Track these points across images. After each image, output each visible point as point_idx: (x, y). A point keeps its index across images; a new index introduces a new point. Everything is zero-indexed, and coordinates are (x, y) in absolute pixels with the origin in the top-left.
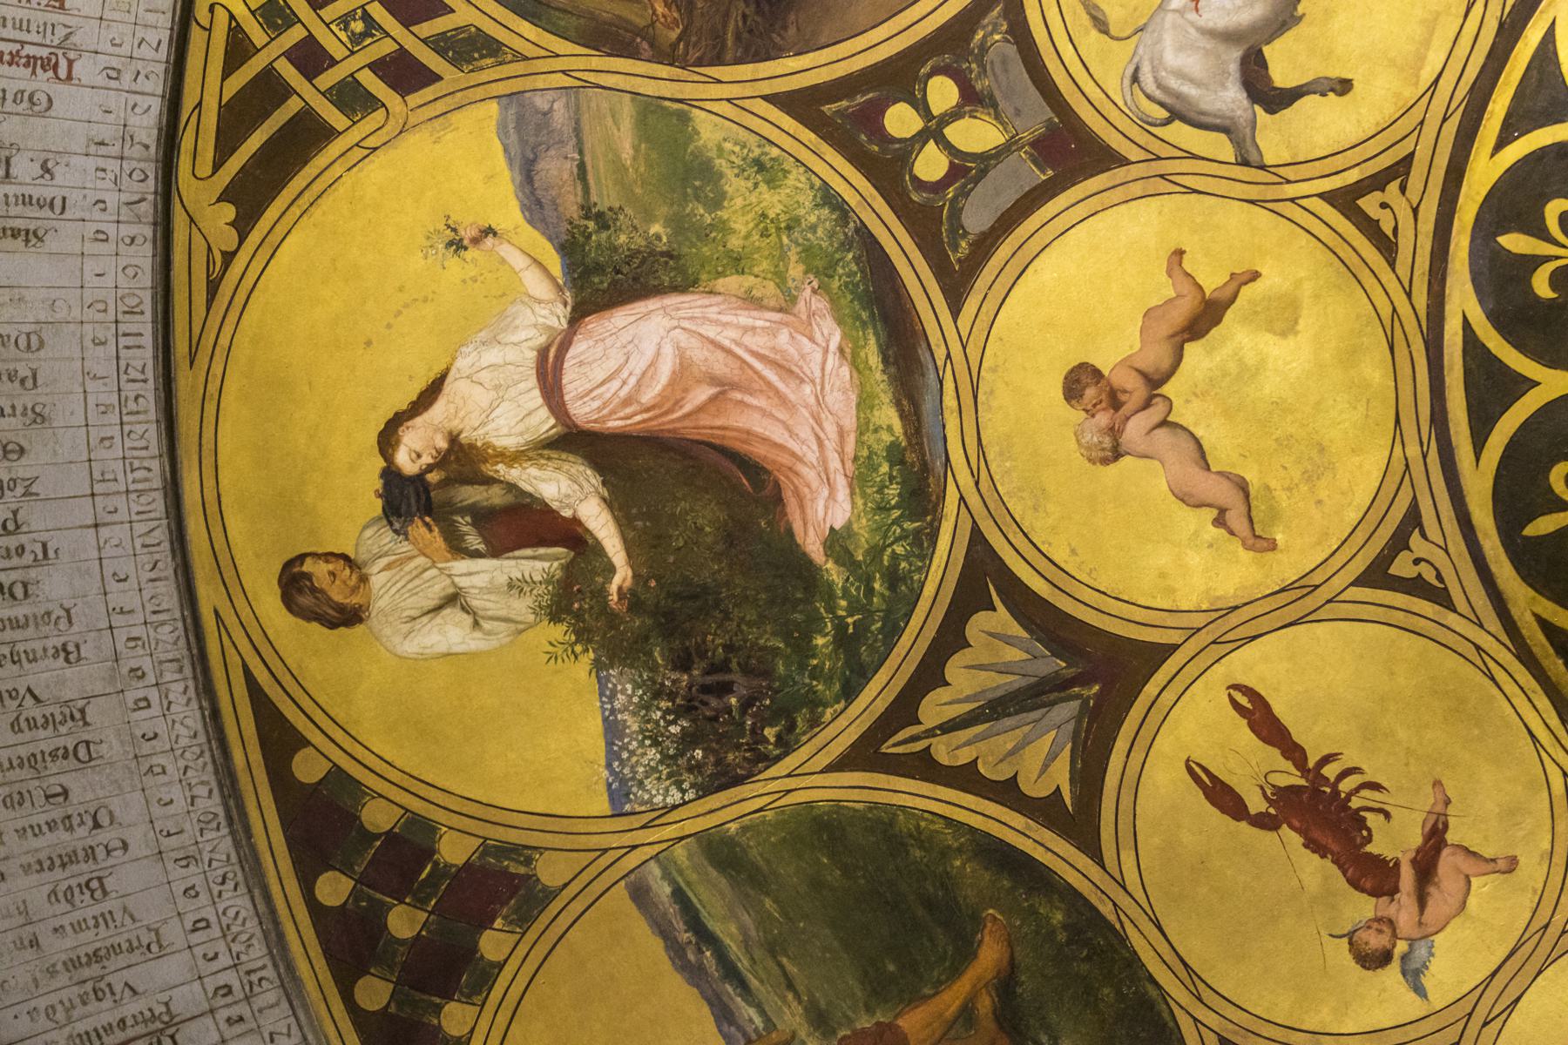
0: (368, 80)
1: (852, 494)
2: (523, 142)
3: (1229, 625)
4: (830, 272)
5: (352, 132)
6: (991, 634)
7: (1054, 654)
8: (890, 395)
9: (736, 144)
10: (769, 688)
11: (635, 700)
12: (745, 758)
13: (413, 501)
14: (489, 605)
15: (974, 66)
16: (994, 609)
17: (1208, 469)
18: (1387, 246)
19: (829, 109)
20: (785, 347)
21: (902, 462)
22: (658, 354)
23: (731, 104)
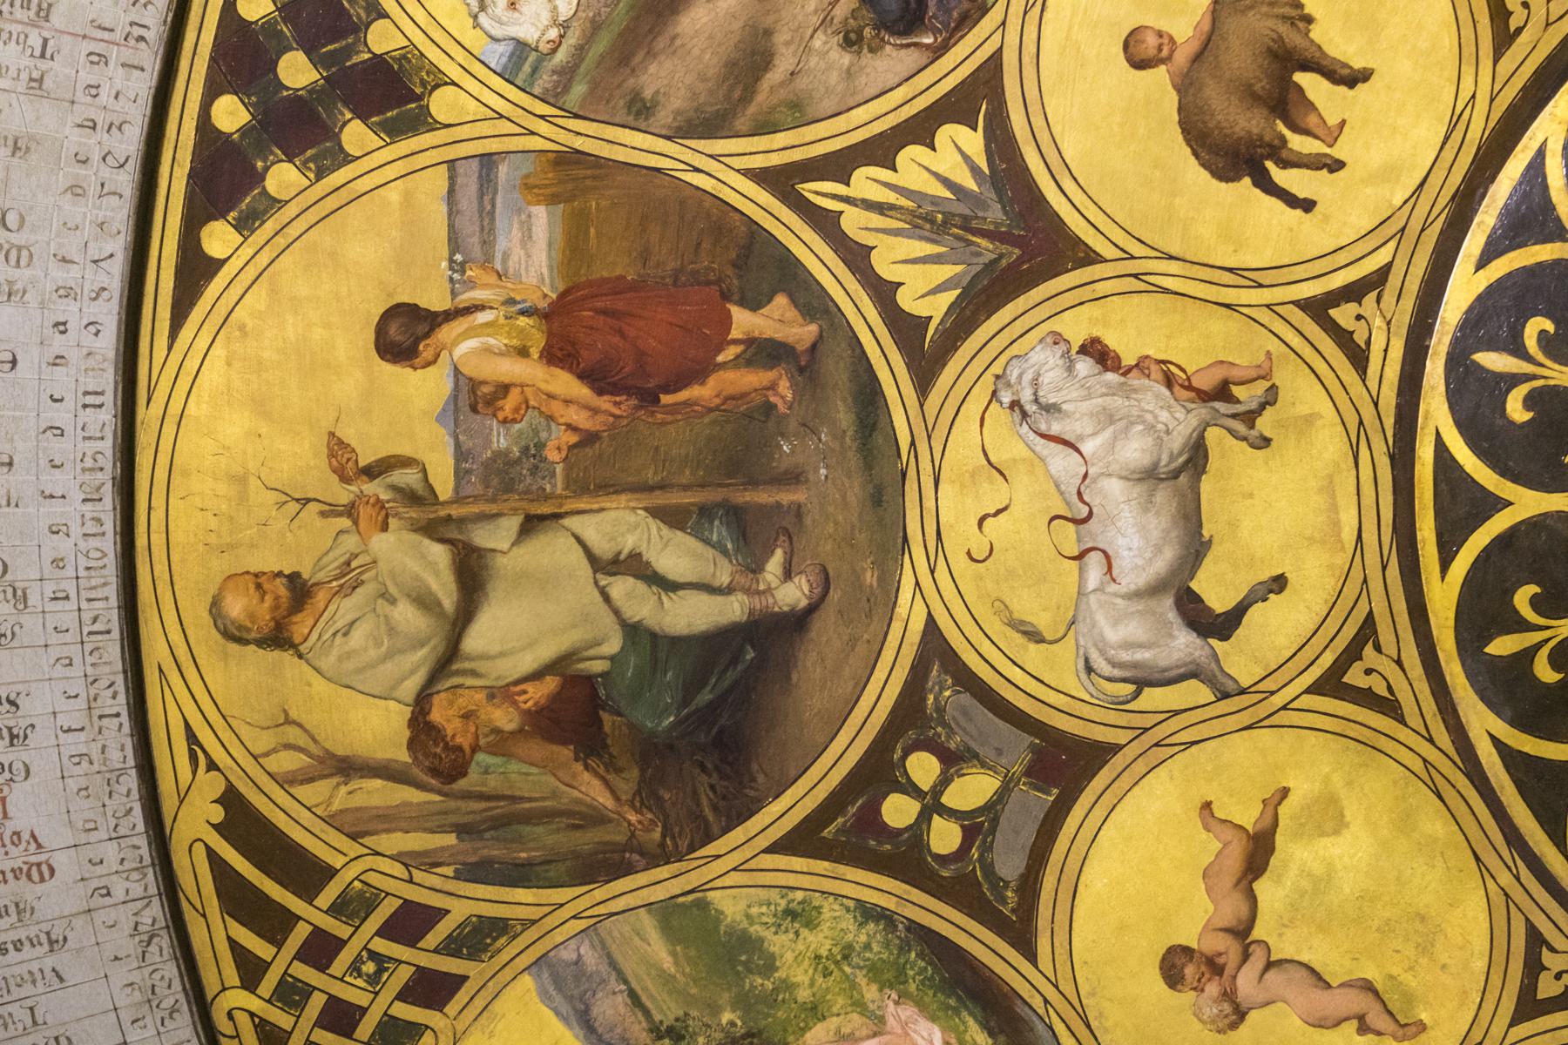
0: (404, 1011)
2: (570, 999)
9: (761, 905)
15: (939, 729)
17: (1329, 986)
18: (1389, 706)
19: (829, 832)
23: (740, 873)
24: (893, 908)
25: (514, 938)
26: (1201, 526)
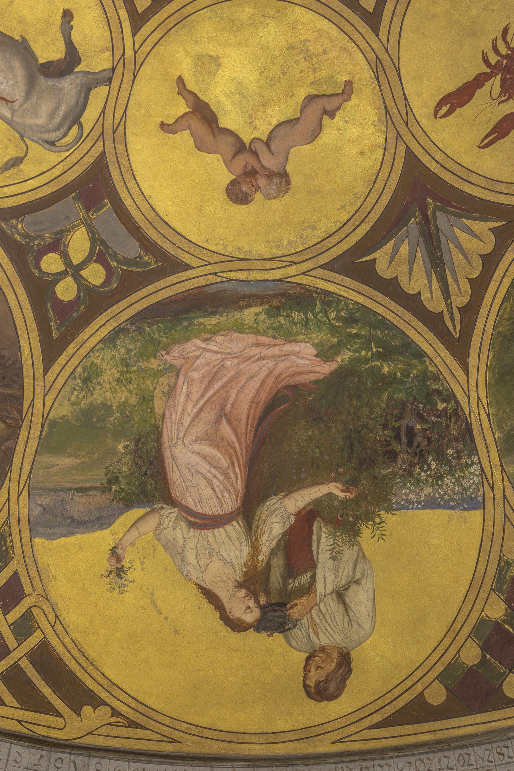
1: (295, 341)
3: (395, 114)
4: (157, 342)
5: (44, 630)
6: (390, 263)
7: (406, 225)
8: (236, 312)
9: (72, 393)
10: (412, 404)
11: (413, 488)
12: (455, 423)
13: (276, 614)
14: (346, 572)
15: (36, 242)
16: (375, 259)
17: (298, 119)
20: (201, 374)
21: (279, 308)
22: (198, 454)
23: (47, 393)
24: (115, 325)
25: (10, 534)
26: (12, 38)
